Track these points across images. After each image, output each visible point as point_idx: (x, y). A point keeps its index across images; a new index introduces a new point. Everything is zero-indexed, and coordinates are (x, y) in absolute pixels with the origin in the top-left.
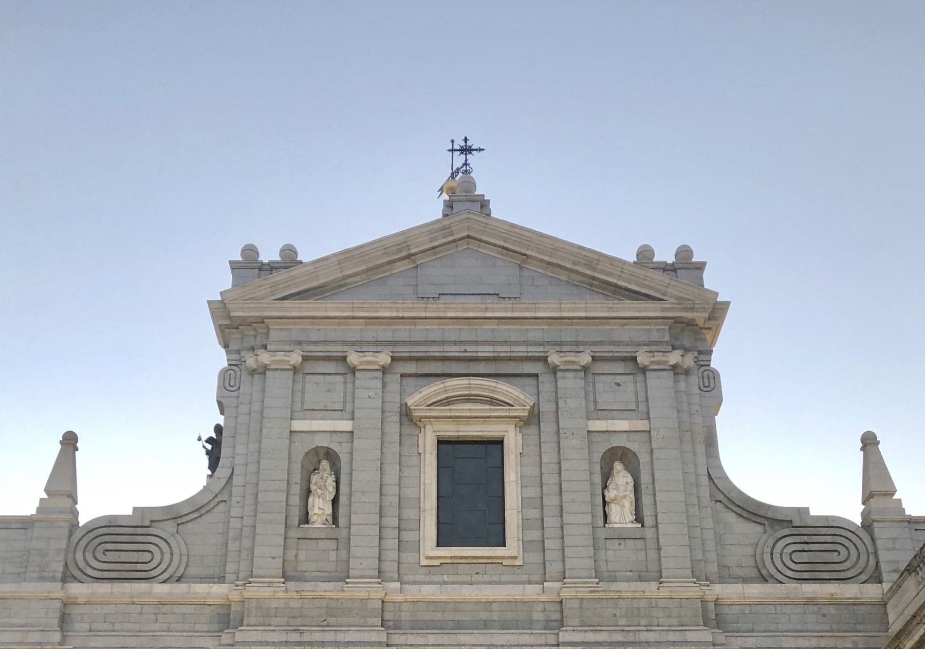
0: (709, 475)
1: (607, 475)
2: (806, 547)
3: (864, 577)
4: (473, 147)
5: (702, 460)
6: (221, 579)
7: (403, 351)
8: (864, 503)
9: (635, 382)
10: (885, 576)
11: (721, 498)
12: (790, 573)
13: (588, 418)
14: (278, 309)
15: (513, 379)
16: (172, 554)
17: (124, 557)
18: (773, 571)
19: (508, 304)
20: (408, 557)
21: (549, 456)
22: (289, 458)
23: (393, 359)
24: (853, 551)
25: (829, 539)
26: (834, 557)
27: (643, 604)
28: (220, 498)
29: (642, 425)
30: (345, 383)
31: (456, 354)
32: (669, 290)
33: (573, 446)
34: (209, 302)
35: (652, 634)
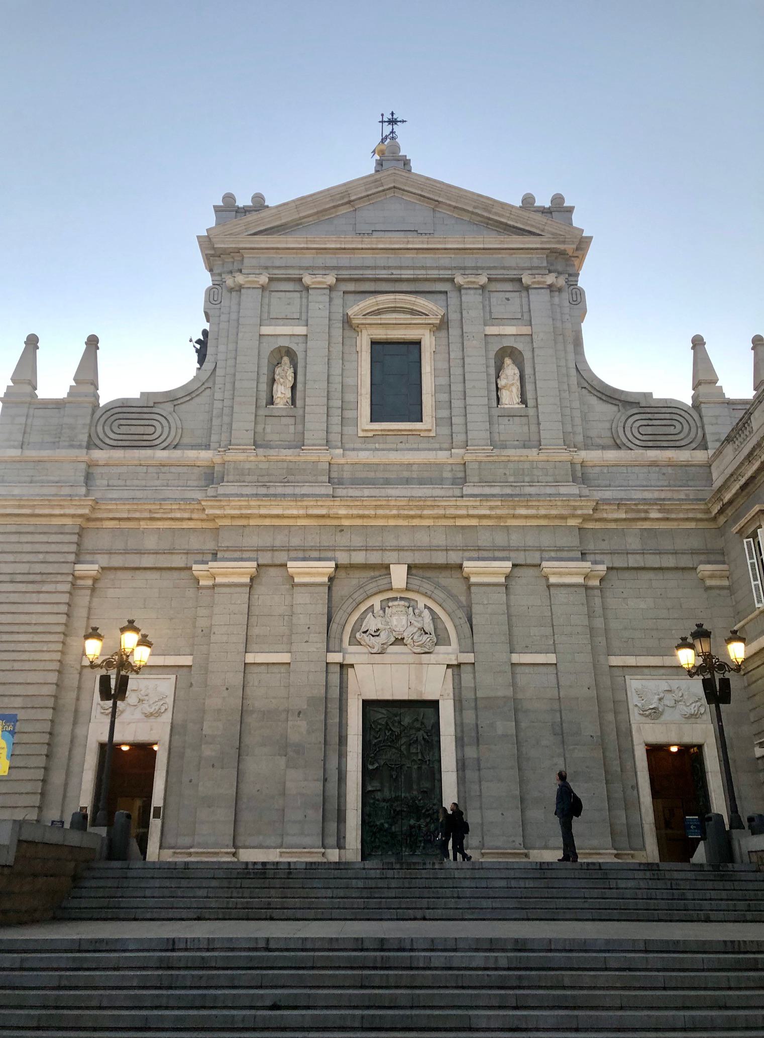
0: (577, 368)
1: (499, 368)
2: (650, 423)
3: (694, 445)
4: (398, 120)
5: (571, 356)
6: (207, 447)
7: (345, 274)
8: (694, 389)
9: (521, 297)
10: (710, 445)
11: (586, 385)
12: (638, 442)
13: (485, 325)
14: (251, 242)
15: (428, 296)
16: (170, 428)
17: (133, 430)
18: (625, 441)
19: (424, 238)
20: (348, 430)
21: (455, 354)
22: (259, 355)
23: (337, 280)
24: (686, 426)
25: (668, 416)
26: (671, 430)
27: (527, 466)
28: (206, 385)
29: (526, 330)
30: (301, 298)
31: (385, 276)
32: (546, 228)
33: (474, 347)
34: (198, 237)
35: (533, 488)
